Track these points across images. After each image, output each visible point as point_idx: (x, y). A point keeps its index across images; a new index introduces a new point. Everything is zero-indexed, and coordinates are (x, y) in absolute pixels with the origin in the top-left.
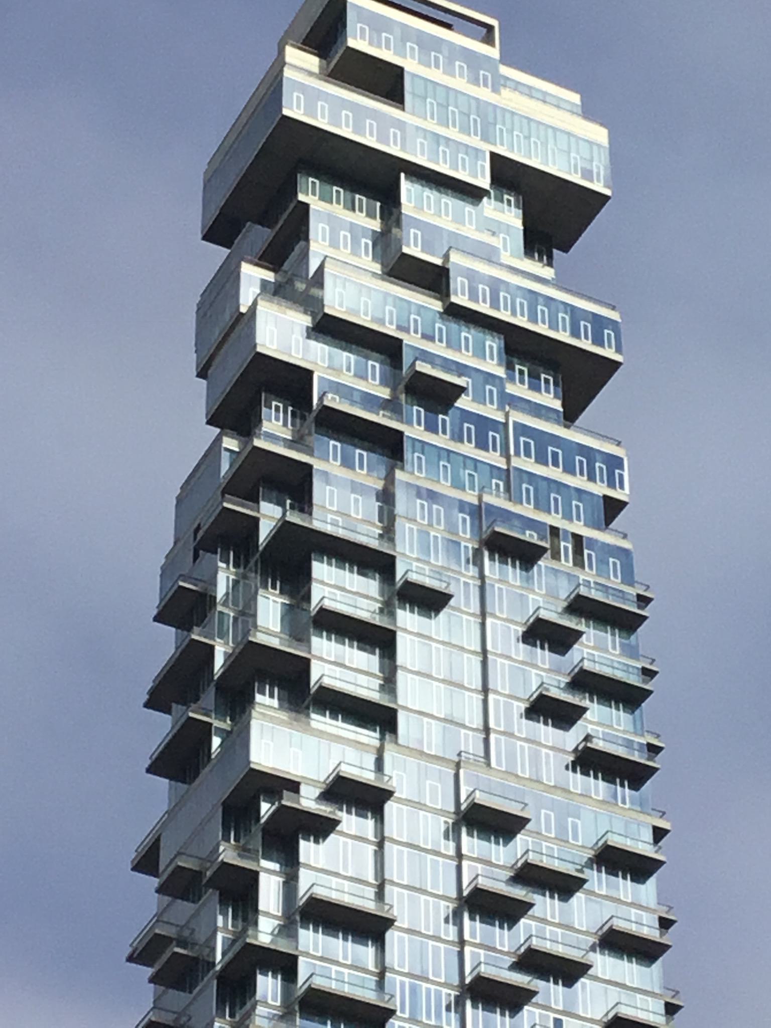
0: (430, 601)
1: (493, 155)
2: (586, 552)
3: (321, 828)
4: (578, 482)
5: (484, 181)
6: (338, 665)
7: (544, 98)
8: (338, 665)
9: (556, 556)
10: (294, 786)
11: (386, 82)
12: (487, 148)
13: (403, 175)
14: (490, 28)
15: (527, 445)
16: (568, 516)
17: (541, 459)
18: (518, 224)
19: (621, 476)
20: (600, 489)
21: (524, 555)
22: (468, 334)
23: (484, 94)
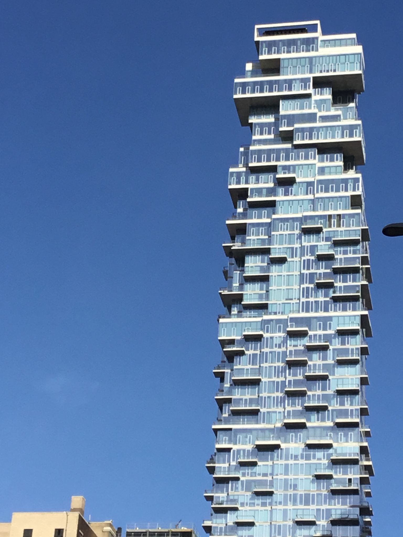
0: (282, 261)
1: (314, 78)
2: (342, 220)
3: (241, 353)
4: (342, 194)
5: (310, 90)
6: (251, 294)
7: (340, 43)
8: (251, 294)
9: (330, 226)
10: (232, 342)
11: (273, 67)
12: (311, 76)
13: (281, 101)
14: (317, 24)
15: (322, 187)
16: (336, 209)
17: (327, 191)
18: (330, 97)
19: (358, 185)
20: (350, 193)
21: (318, 231)
22: (302, 153)
23: (312, 54)
